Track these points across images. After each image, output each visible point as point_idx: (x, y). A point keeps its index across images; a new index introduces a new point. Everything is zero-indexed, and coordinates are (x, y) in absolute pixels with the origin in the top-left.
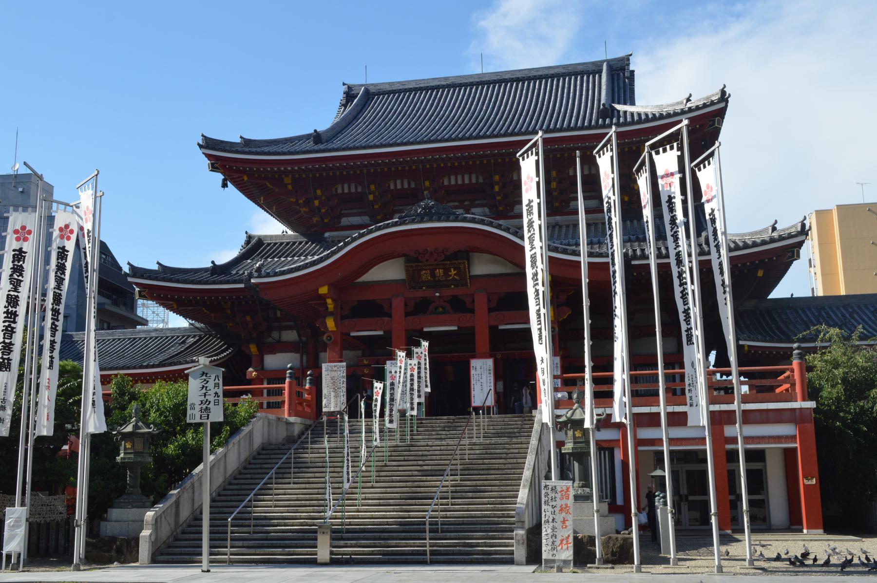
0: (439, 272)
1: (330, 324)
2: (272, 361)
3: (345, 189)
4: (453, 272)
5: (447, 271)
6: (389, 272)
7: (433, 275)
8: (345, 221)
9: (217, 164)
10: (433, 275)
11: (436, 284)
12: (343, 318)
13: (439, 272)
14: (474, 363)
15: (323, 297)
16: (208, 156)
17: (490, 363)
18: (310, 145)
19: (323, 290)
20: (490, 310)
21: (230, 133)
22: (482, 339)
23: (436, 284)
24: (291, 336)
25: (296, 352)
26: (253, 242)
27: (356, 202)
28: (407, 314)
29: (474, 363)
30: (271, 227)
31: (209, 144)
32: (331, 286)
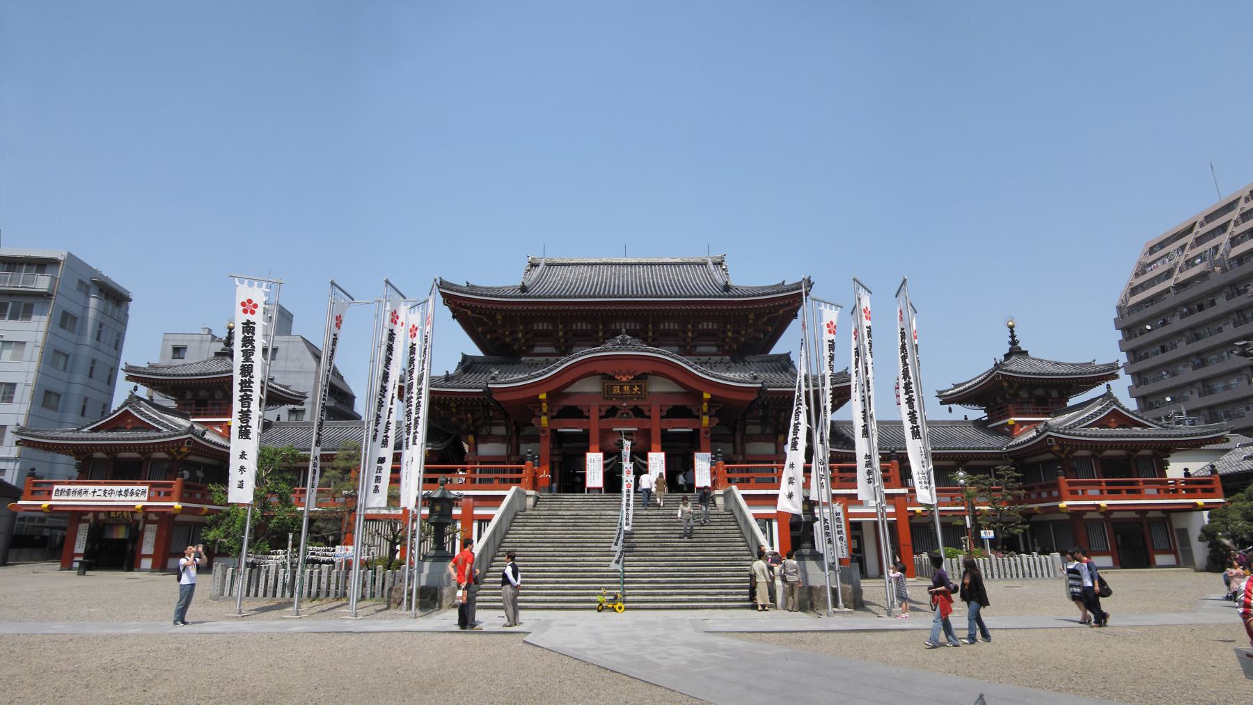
0: (626, 388)
1: (544, 420)
2: (485, 449)
3: (540, 326)
4: (636, 389)
5: (632, 388)
6: (590, 387)
7: (621, 389)
8: (537, 350)
9: (449, 300)
10: (621, 389)
11: (622, 397)
12: (552, 418)
13: (626, 388)
14: (650, 454)
15: (540, 401)
16: (442, 294)
17: (662, 455)
18: (518, 293)
19: (543, 396)
20: (662, 417)
21: (459, 279)
22: (656, 436)
23: (622, 397)
24: (500, 430)
25: (503, 442)
26: (468, 363)
27: (546, 336)
28: (601, 418)
29: (650, 454)
30: (475, 351)
31: (442, 284)
32: (548, 394)
